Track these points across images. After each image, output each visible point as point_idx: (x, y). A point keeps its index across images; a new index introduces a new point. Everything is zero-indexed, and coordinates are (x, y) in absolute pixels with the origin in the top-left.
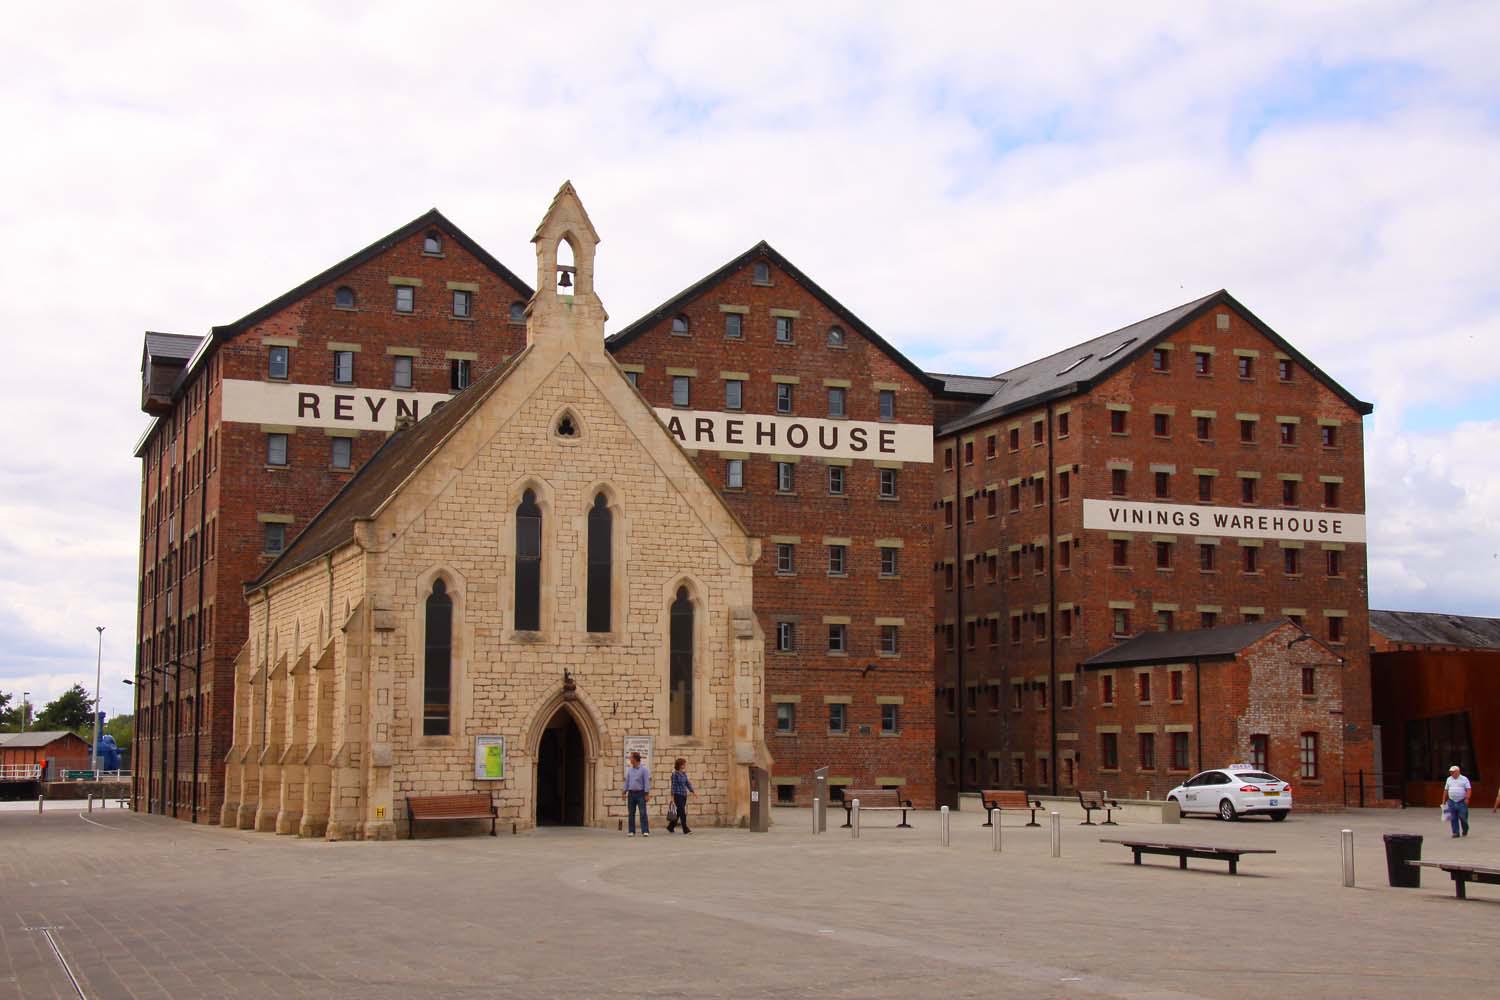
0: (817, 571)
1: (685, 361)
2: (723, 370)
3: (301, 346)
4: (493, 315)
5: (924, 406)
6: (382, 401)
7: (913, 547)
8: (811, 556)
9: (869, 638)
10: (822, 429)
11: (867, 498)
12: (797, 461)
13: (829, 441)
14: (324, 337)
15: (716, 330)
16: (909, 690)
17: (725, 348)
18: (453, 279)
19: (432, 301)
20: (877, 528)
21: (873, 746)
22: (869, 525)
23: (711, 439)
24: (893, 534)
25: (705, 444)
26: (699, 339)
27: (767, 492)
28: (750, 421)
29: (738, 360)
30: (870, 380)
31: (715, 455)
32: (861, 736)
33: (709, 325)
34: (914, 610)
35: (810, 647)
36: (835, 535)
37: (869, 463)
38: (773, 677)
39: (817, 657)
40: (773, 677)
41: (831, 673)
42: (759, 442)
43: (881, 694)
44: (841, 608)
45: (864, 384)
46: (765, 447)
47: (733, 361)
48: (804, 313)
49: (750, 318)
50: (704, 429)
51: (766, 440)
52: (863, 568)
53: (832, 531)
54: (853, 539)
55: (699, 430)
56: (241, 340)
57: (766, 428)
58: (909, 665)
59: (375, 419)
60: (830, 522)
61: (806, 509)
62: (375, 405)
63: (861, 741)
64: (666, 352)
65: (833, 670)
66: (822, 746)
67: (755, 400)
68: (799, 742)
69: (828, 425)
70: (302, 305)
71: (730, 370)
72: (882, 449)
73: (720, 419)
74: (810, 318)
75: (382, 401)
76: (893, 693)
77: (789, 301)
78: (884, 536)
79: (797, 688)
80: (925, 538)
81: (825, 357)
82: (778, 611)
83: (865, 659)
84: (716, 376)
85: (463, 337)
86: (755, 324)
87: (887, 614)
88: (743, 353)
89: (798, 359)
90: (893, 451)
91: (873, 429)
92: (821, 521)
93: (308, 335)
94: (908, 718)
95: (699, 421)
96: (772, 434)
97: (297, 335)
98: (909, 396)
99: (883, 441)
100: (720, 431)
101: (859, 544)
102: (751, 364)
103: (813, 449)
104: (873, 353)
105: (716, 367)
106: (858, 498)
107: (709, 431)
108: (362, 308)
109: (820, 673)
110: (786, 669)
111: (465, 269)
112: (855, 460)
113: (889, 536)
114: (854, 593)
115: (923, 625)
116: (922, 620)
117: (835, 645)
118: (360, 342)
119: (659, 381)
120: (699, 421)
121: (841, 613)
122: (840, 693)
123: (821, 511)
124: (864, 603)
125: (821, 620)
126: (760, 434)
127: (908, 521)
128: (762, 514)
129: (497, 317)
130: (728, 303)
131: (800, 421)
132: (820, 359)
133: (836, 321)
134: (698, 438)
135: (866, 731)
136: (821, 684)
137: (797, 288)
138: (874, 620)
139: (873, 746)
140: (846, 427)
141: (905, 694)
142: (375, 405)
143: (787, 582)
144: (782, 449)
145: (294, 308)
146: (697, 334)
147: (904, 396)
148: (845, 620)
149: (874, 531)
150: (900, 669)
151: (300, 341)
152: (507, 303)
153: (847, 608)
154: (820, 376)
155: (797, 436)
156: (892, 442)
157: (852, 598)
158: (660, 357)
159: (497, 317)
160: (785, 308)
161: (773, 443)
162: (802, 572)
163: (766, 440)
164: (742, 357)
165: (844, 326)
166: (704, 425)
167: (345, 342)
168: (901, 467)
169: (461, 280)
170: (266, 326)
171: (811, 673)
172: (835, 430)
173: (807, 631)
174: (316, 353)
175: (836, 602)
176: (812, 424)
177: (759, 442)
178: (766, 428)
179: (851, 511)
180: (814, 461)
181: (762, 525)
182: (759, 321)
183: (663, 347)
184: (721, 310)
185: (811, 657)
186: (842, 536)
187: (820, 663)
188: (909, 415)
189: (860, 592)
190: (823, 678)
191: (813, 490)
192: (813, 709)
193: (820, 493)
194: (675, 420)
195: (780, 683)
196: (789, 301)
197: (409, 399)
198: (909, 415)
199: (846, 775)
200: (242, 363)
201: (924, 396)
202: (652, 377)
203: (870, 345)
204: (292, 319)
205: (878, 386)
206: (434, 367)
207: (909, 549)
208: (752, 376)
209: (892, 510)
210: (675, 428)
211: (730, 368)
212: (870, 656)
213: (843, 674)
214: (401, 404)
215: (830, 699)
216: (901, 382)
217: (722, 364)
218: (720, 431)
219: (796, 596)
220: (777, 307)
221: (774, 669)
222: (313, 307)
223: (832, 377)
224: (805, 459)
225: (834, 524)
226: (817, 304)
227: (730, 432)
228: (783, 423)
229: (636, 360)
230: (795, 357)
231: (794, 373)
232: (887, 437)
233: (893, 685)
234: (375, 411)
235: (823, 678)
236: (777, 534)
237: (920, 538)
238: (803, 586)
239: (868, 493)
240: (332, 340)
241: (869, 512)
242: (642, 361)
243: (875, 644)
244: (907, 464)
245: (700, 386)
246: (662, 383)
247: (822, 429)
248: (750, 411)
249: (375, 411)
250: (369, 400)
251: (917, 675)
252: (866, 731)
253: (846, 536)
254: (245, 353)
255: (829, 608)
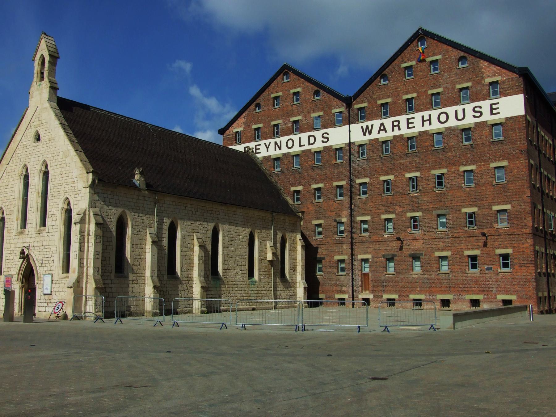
0: (457, 185)
1: (386, 96)
2: (404, 95)
3: (245, 129)
4: (307, 98)
5: (517, 84)
6: (270, 143)
7: (514, 164)
8: (453, 178)
9: (489, 218)
10: (456, 111)
11: (484, 142)
12: (443, 130)
13: (460, 116)
14: (251, 124)
15: (400, 77)
16: (515, 245)
17: (404, 85)
18: (292, 89)
19: (286, 100)
20: (491, 157)
21: (495, 277)
22: (486, 156)
23: (399, 129)
24: (501, 159)
25: (397, 132)
26: (392, 83)
27: (428, 150)
28: (418, 116)
29: (411, 88)
30: (483, 78)
31: (401, 136)
32: (487, 272)
33: (396, 75)
34: (517, 199)
35: (455, 226)
36: (466, 165)
37: (484, 123)
38: (436, 243)
39: (459, 231)
40: (436, 243)
41: (468, 239)
42: (423, 125)
43: (499, 248)
44: (471, 203)
45: (479, 82)
46: (427, 127)
47: (409, 89)
48: (444, 55)
49: (416, 66)
50: (396, 125)
51: (427, 123)
52: (484, 180)
53: (464, 163)
54: (477, 166)
55: (393, 126)
56: (227, 132)
57: (426, 118)
58: (514, 231)
59: (267, 151)
60: (463, 158)
61: (449, 154)
62: (267, 146)
63: (487, 275)
64: (377, 94)
65: (468, 237)
66: (464, 278)
67: (420, 105)
68: (451, 276)
69: (459, 108)
70: (244, 114)
71: (407, 94)
72: (492, 114)
73: (403, 119)
74: (447, 56)
75: (270, 143)
76: (506, 248)
77: (436, 52)
78: (496, 161)
79: (449, 248)
80: (521, 157)
81: (456, 74)
82: (436, 209)
83: (487, 229)
84: (401, 98)
85: (296, 111)
86: (419, 68)
87: (499, 204)
88: (414, 84)
89: (441, 79)
90: (499, 113)
91: (485, 105)
92: (458, 159)
93: (246, 125)
94: (516, 261)
95: (393, 122)
96: (430, 120)
97: (243, 126)
98: (507, 81)
99: (492, 109)
100: (403, 125)
101: (481, 168)
102: (417, 88)
103: (452, 123)
104: (484, 64)
105: (400, 94)
106: (479, 143)
107: (398, 126)
108: (263, 110)
109: (461, 239)
110: (442, 238)
111: (297, 83)
112: (476, 123)
113: (499, 160)
114: (478, 194)
115: (523, 207)
116: (523, 205)
117: (471, 223)
118: (262, 123)
119: (374, 108)
120: (393, 122)
121: (471, 206)
122: (473, 249)
123: (458, 154)
124: (485, 199)
125: (460, 211)
126: (423, 121)
127: (510, 150)
128: (426, 161)
129: (308, 99)
130: (405, 62)
131: (444, 110)
132: (453, 76)
133: (462, 54)
134: (393, 130)
135: (489, 269)
136: (462, 245)
137: (439, 44)
138: (491, 208)
139: (495, 277)
140: (469, 107)
141: (514, 247)
142: (267, 146)
143: (441, 193)
144: (436, 126)
145: (243, 116)
146: (391, 81)
147: (504, 82)
148: (475, 209)
149: (489, 159)
150: (510, 234)
151: (244, 128)
152: (312, 92)
153: (476, 203)
154: (454, 84)
155: (443, 118)
156: (498, 108)
157: (478, 197)
158: (374, 97)
159: (308, 99)
160: (434, 56)
161: (430, 124)
162: (449, 186)
163: (427, 123)
164: (413, 86)
165: (466, 55)
166: (396, 123)
167: (258, 124)
168: (504, 121)
169: (295, 88)
170: (234, 125)
171: (457, 239)
172: (464, 110)
173: (453, 217)
174: (249, 131)
175: (469, 201)
176: (451, 110)
177: (423, 125)
178: (426, 118)
179: (475, 151)
180: (452, 128)
181: (427, 167)
182: (420, 66)
183: (375, 92)
184: (402, 67)
185: (455, 231)
186: (470, 165)
187: (461, 234)
188: (508, 92)
189: (482, 194)
190: (463, 242)
191: (453, 144)
192: (458, 259)
193: (457, 144)
194: (382, 124)
195: (439, 246)
196: (436, 52)
197: (278, 140)
198: (508, 92)
199: (478, 294)
200: (228, 141)
201: (517, 79)
202: (371, 107)
203: (482, 61)
204: (241, 120)
205: (488, 80)
206: (287, 126)
207: (512, 166)
208: (418, 93)
209: (499, 145)
210: (382, 128)
211: (407, 93)
212: (490, 228)
213: (475, 238)
214: (276, 143)
215: (467, 253)
216: (501, 75)
217: (404, 92)
218: (403, 125)
219: (446, 200)
220: (430, 57)
221: (435, 238)
222: (248, 114)
223: (460, 83)
224: (447, 129)
225: (465, 159)
226: (450, 48)
227: (408, 123)
228: (434, 113)
229: (364, 101)
230: (440, 79)
231: (439, 87)
232: (494, 107)
233: (506, 243)
234: (267, 148)
235: (463, 242)
236: (435, 169)
237: (518, 158)
238: (449, 194)
239: (485, 139)
240: (254, 125)
241: (486, 149)
242: (366, 101)
243: (493, 221)
244: (507, 119)
245: (393, 105)
246: (376, 109)
247: (456, 111)
248: (417, 111)
249: (267, 148)
250: (265, 144)
251: (521, 236)
252: (489, 269)
253: (473, 164)
254: (228, 137)
255: (464, 204)
